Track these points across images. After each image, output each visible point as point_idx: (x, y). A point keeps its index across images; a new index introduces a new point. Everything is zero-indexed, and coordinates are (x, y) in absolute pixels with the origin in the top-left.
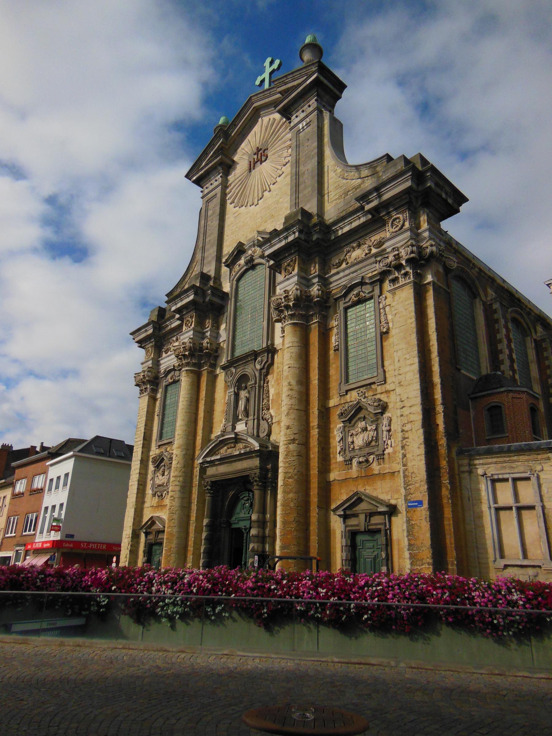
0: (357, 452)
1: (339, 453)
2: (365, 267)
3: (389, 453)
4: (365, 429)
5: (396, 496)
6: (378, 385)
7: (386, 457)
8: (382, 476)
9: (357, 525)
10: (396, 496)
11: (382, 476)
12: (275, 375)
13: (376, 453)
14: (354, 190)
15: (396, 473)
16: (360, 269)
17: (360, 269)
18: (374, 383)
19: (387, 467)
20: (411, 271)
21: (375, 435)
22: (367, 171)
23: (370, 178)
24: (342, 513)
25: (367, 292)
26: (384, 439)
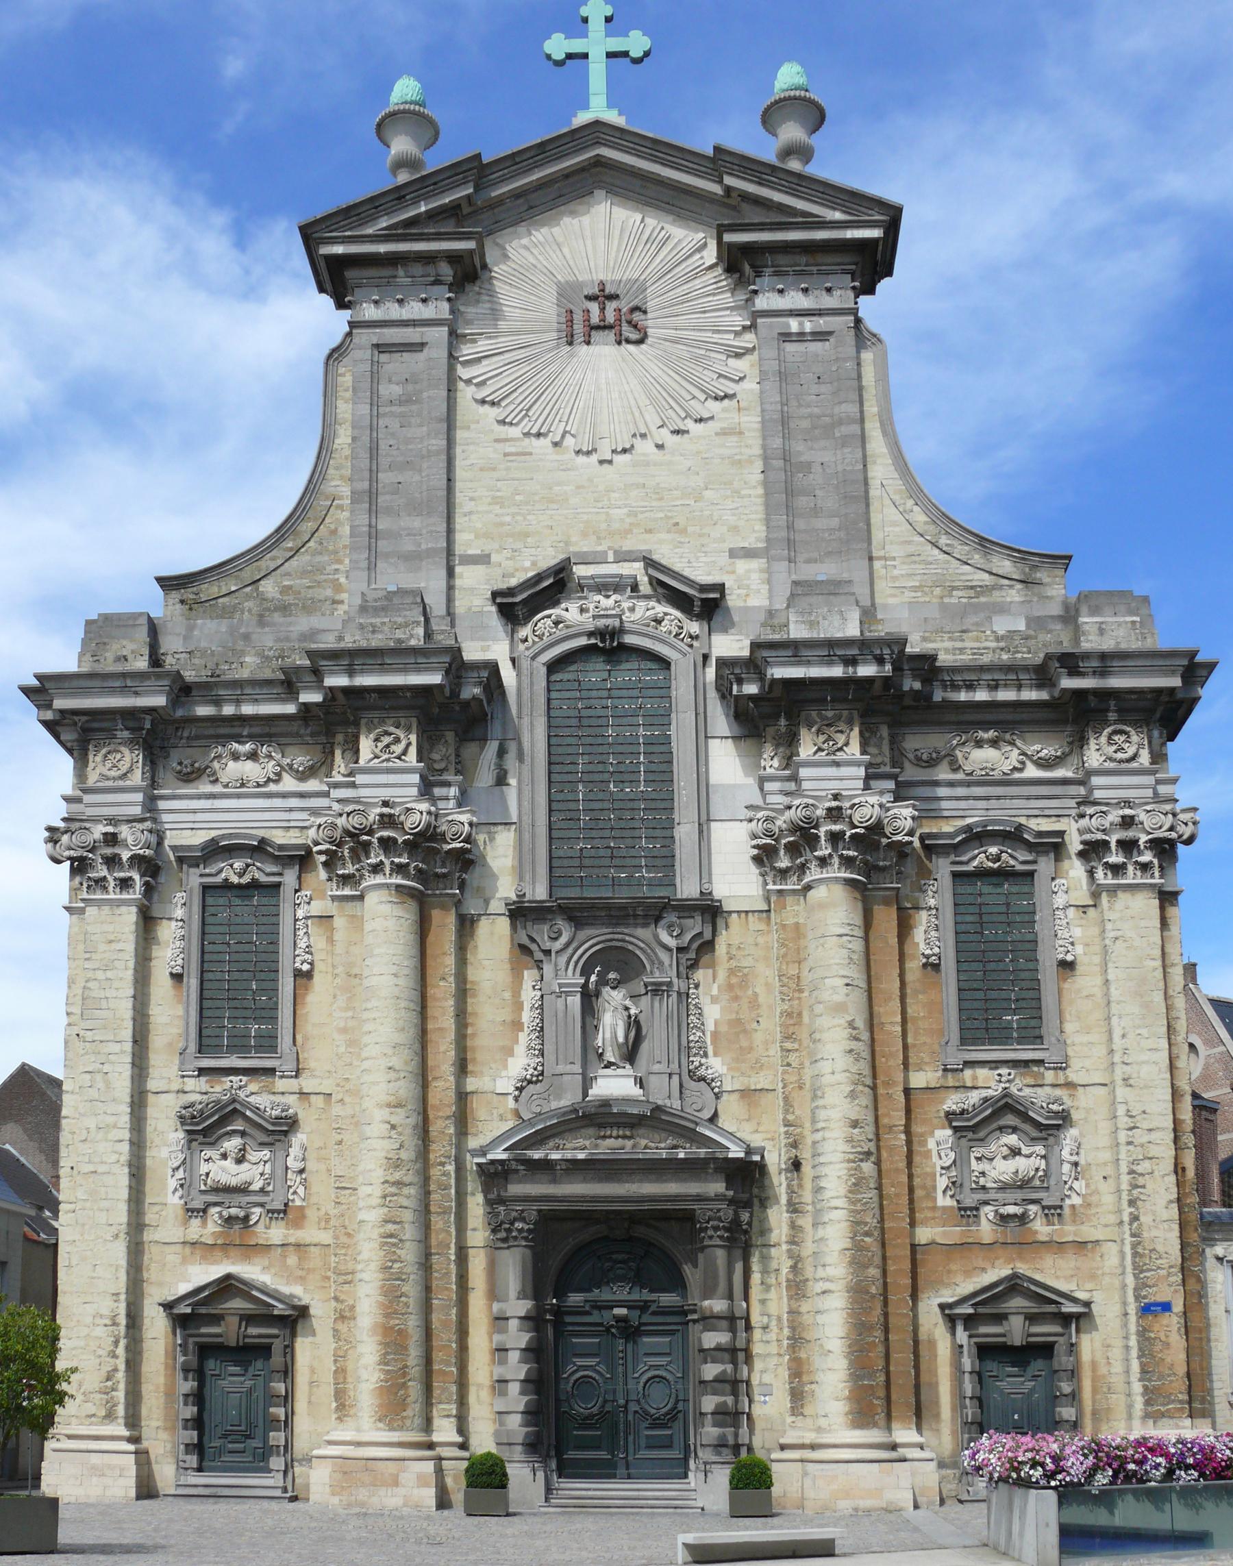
0: (992, 1195)
1: (944, 1192)
2: (1012, 798)
3: (1073, 1206)
4: (1015, 1152)
5: (1089, 1286)
6: (1049, 1069)
7: (1067, 1211)
8: (1057, 1246)
9: (1004, 1335)
10: (1089, 1286)
11: (1057, 1246)
12: (722, 974)
13: (1044, 1203)
14: (972, 593)
15: (1090, 1246)
16: (998, 798)
17: (998, 798)
18: (1040, 1062)
19: (1069, 1232)
20: (1156, 861)
21: (1043, 1166)
22: (1007, 563)
23: (1019, 586)
24: (971, 1311)
25: (1021, 858)
26: (1064, 1178)
